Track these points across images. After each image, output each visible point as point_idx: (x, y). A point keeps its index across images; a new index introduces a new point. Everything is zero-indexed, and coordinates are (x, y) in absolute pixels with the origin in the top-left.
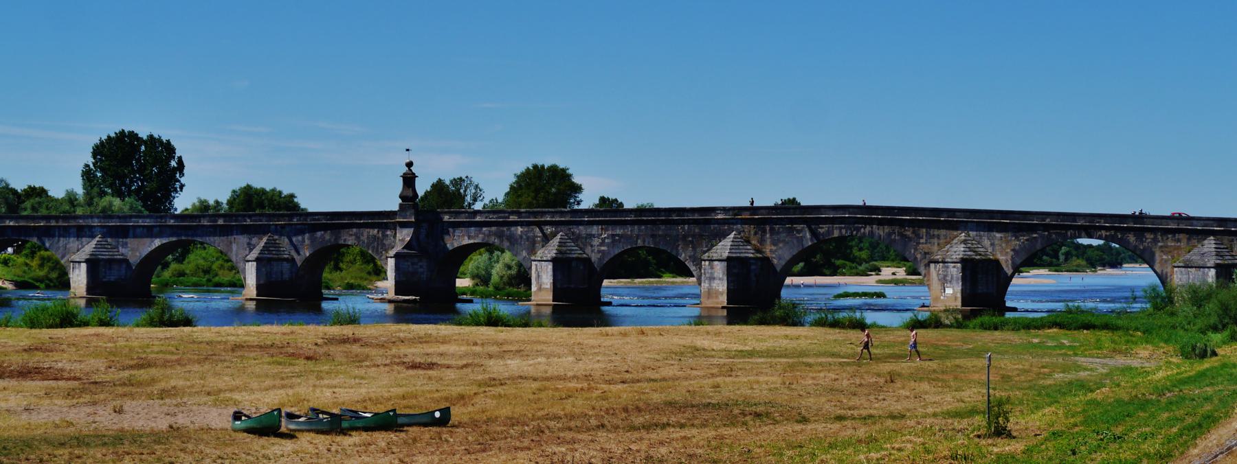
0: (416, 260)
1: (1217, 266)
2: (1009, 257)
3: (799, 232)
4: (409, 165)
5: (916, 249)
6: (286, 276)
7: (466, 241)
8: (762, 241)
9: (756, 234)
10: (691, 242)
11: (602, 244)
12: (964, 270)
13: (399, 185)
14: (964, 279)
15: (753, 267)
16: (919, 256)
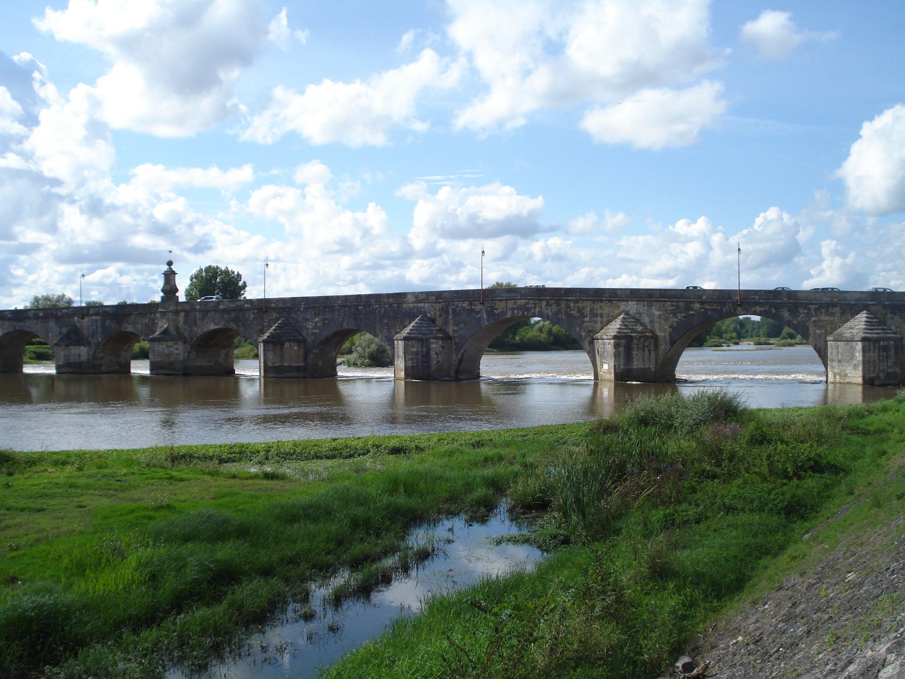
0: (171, 343)
1: (864, 340)
2: (667, 334)
3: (477, 313)
4: (170, 263)
5: (581, 328)
6: (84, 358)
7: (213, 327)
8: (446, 322)
9: (440, 316)
10: (387, 324)
11: (314, 328)
12: (616, 346)
13: (161, 283)
14: (616, 355)
15: (433, 346)
16: (583, 334)
